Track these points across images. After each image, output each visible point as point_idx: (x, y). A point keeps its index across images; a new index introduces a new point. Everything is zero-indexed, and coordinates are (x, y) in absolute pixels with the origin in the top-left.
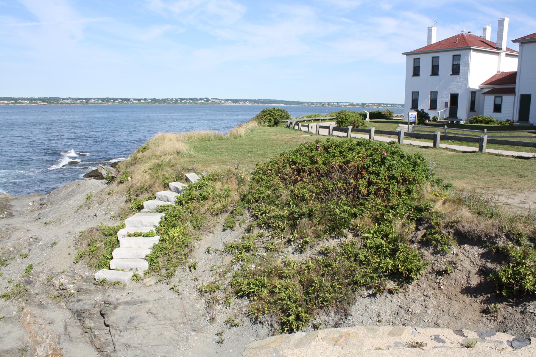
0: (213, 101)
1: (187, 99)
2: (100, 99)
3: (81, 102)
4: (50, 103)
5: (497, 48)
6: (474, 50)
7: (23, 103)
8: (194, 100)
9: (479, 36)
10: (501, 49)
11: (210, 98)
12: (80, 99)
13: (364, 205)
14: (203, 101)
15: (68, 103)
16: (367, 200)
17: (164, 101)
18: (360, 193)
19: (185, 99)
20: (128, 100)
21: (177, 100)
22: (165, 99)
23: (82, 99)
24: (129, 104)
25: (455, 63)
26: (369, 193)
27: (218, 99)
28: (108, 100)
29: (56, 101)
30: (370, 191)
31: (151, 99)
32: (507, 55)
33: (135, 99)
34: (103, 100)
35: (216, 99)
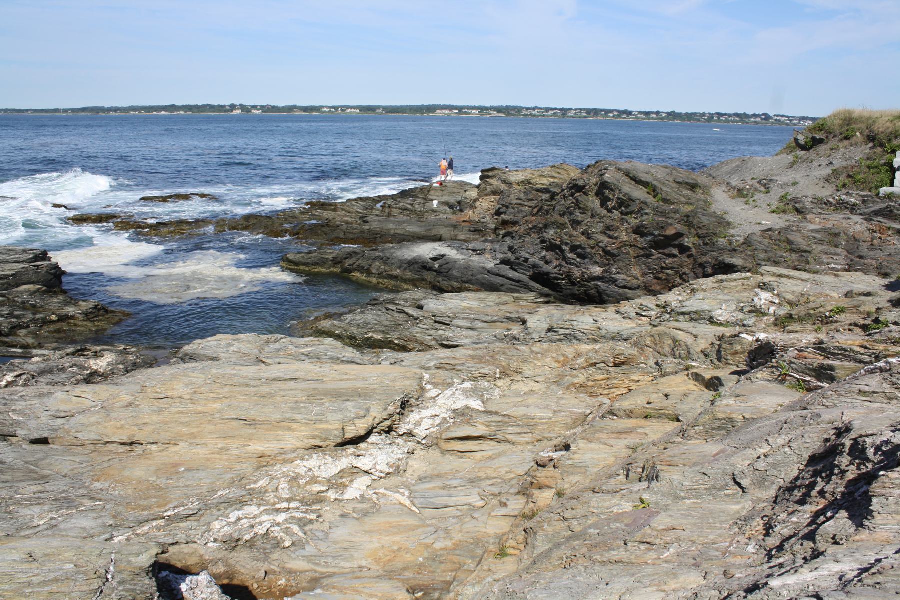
0: (776, 120)
1: (730, 115)
2: (584, 110)
3: (555, 113)
4: (509, 114)
7: (470, 114)
8: (743, 117)
11: (772, 114)
12: (552, 109)
14: (758, 120)
15: (534, 116)
17: (690, 117)
19: (726, 114)
20: (629, 113)
21: (711, 116)
22: (692, 114)
23: (556, 109)
24: (631, 119)
27: (787, 117)
28: (596, 112)
29: (517, 112)
31: (667, 113)
33: (640, 113)
34: (589, 112)
35: (783, 116)
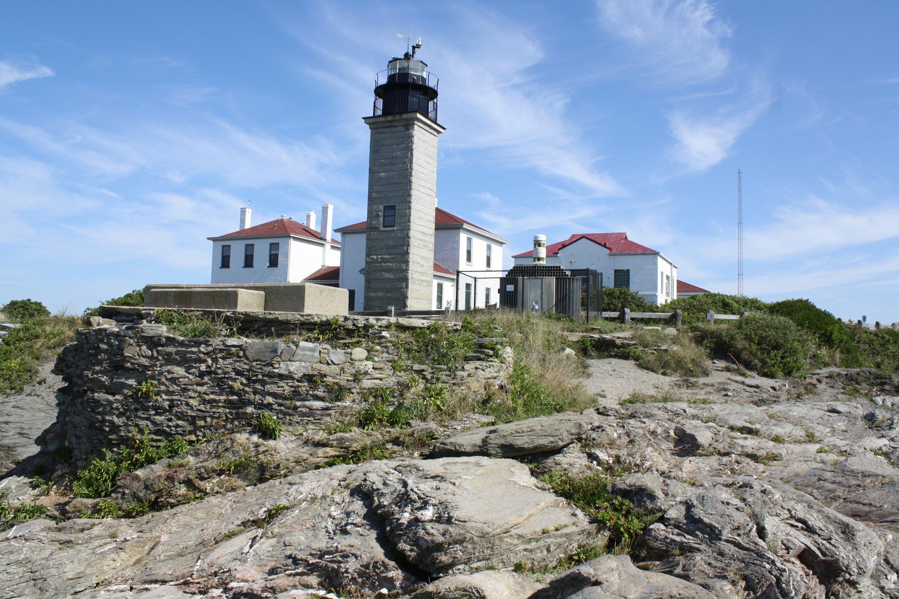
5: (321, 239)
6: (294, 238)
10: (325, 240)
25: (272, 253)
32: (332, 247)
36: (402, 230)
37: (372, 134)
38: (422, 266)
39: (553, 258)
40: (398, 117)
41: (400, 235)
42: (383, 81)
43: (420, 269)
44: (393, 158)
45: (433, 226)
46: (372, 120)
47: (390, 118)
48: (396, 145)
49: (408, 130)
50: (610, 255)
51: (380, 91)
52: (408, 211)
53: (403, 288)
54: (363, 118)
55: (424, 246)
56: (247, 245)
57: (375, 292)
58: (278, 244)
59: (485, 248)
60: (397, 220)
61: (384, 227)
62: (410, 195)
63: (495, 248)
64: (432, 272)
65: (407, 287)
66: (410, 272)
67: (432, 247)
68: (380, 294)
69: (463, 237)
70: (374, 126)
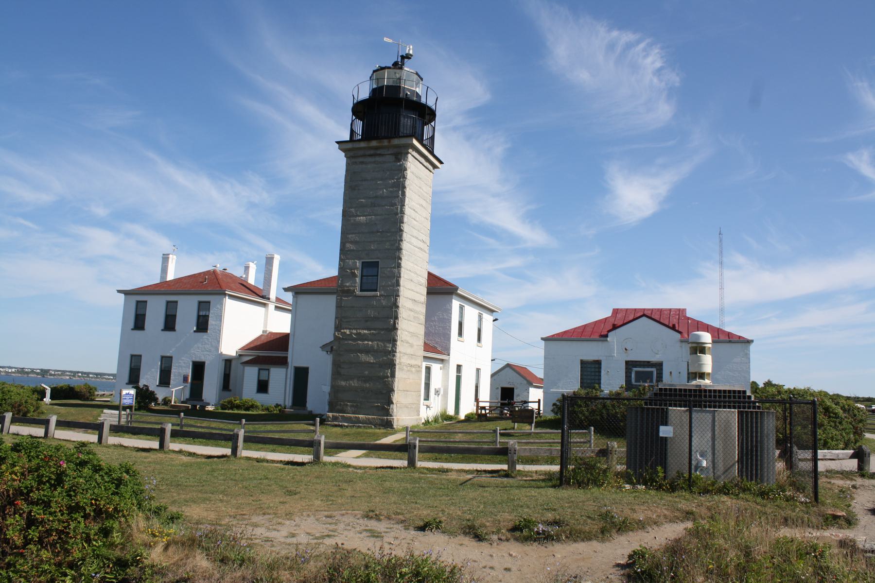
5: (263, 297)
6: (231, 297)
9: (239, 276)
10: (269, 299)
13: (15, 567)
16: (22, 555)
18: (8, 543)
25: (201, 313)
26: (27, 542)
30: (30, 537)
32: (277, 308)
36: (387, 297)
37: (348, 165)
38: (412, 346)
39: (600, 343)
40: (385, 142)
41: (384, 303)
42: (365, 94)
43: (409, 351)
44: (376, 197)
45: (424, 291)
46: (349, 146)
47: (374, 143)
48: (382, 179)
49: (399, 160)
50: (682, 341)
51: (360, 109)
52: (396, 270)
53: (388, 377)
54: (337, 142)
55: (415, 318)
56: (168, 302)
57: (346, 380)
58: (209, 302)
59: (477, 319)
60: (381, 283)
61: (361, 290)
62: (399, 249)
63: (488, 318)
64: (422, 353)
65: (393, 375)
66: (398, 355)
67: (422, 318)
68: (354, 383)
69: (456, 304)
70: (352, 154)
